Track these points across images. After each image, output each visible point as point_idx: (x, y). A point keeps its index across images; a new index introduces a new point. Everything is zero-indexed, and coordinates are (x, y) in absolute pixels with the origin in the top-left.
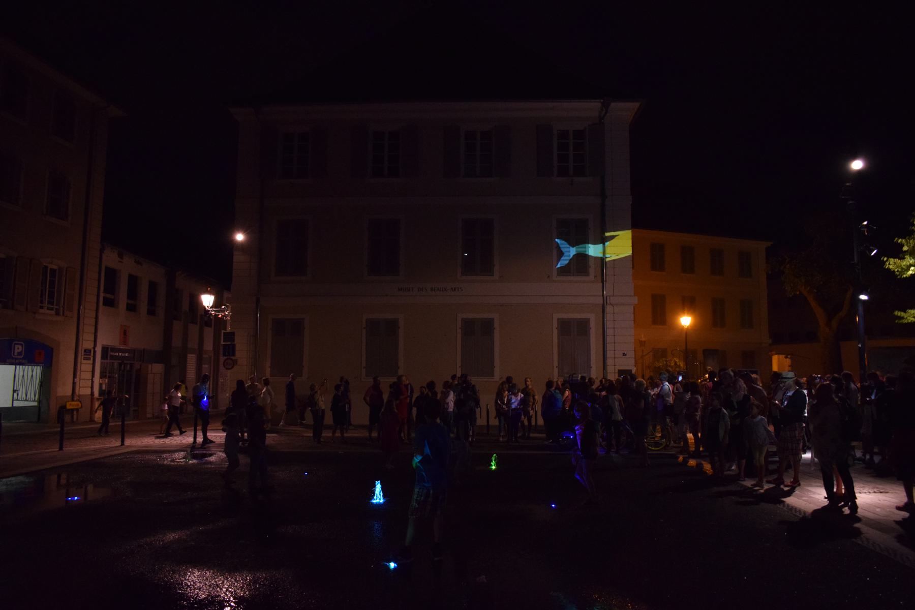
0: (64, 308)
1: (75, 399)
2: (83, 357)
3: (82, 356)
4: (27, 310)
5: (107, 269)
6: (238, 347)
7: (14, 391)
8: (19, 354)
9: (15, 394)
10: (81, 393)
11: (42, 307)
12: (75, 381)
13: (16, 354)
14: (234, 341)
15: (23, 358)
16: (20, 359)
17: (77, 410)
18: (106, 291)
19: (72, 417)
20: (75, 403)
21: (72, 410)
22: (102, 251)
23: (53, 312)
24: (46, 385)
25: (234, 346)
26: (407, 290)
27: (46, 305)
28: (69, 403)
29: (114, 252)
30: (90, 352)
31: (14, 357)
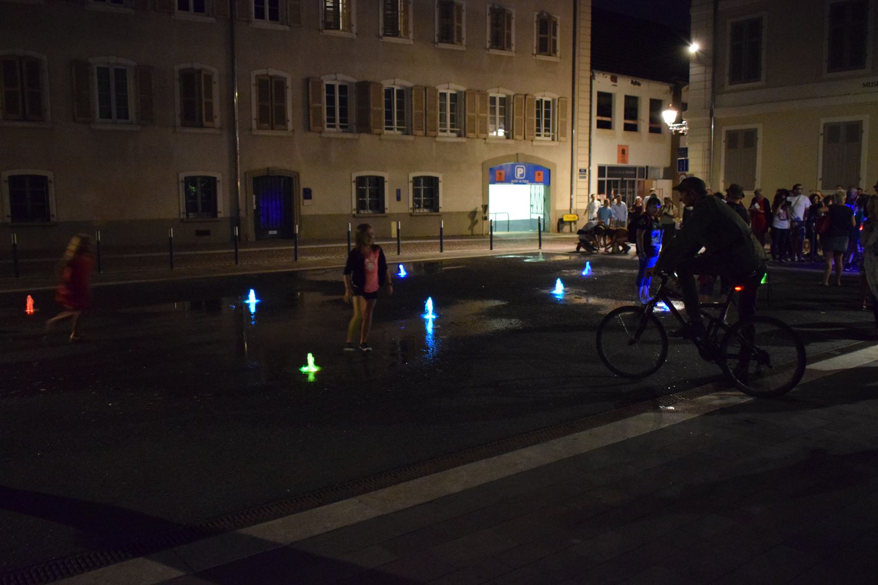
0: (558, 134)
1: (572, 212)
2: (578, 176)
3: (577, 175)
4: (525, 139)
5: (600, 95)
6: (690, 163)
7: (531, 206)
8: (522, 175)
9: (532, 208)
10: (578, 208)
11: (539, 135)
12: (572, 197)
13: (519, 175)
14: (686, 156)
15: (526, 179)
16: (524, 179)
17: (575, 222)
18: (599, 114)
19: (571, 227)
20: (572, 216)
21: (570, 222)
22: (592, 78)
23: (550, 139)
24: (547, 199)
25: (687, 161)
26: (874, 85)
27: (543, 133)
28: (566, 216)
29: (606, 77)
30: (585, 171)
31: (517, 178)
